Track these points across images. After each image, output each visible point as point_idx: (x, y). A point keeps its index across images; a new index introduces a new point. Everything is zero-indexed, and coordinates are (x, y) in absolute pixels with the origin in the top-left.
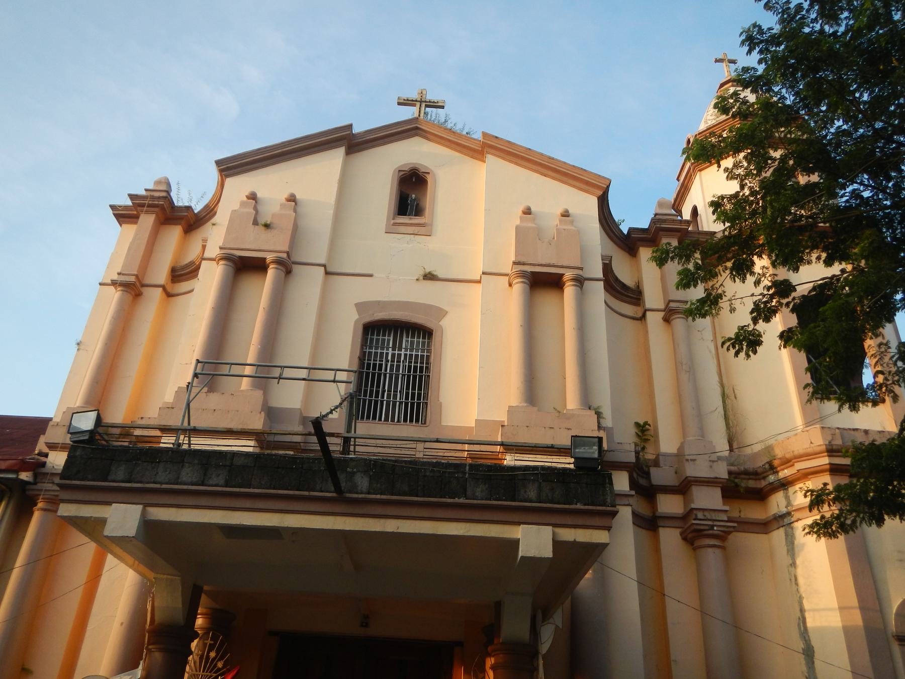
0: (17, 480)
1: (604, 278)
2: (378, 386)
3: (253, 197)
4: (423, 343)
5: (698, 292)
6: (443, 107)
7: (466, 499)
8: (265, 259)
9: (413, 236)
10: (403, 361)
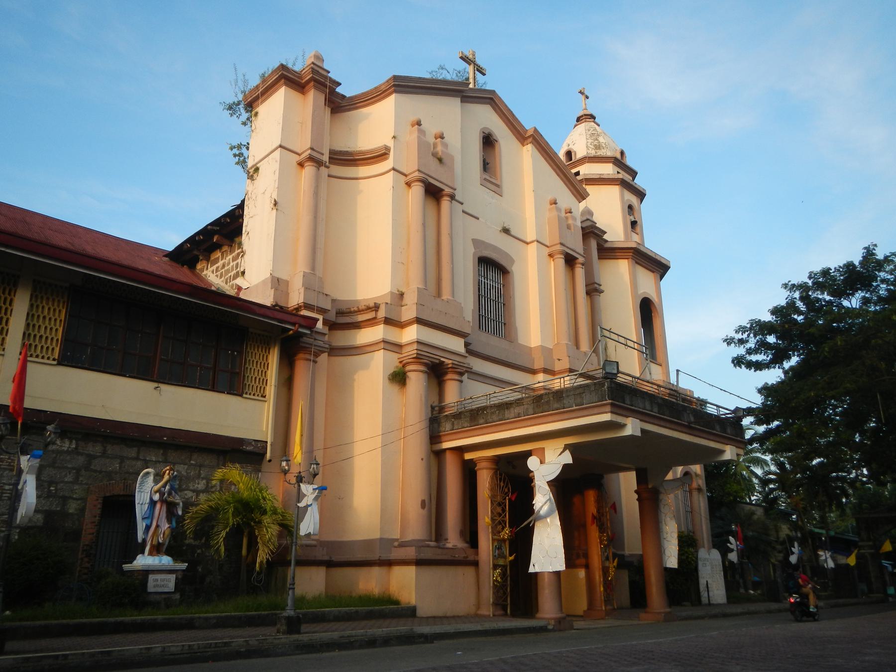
5: (739, 336)
6: (484, 74)
8: (442, 190)
9: (494, 193)
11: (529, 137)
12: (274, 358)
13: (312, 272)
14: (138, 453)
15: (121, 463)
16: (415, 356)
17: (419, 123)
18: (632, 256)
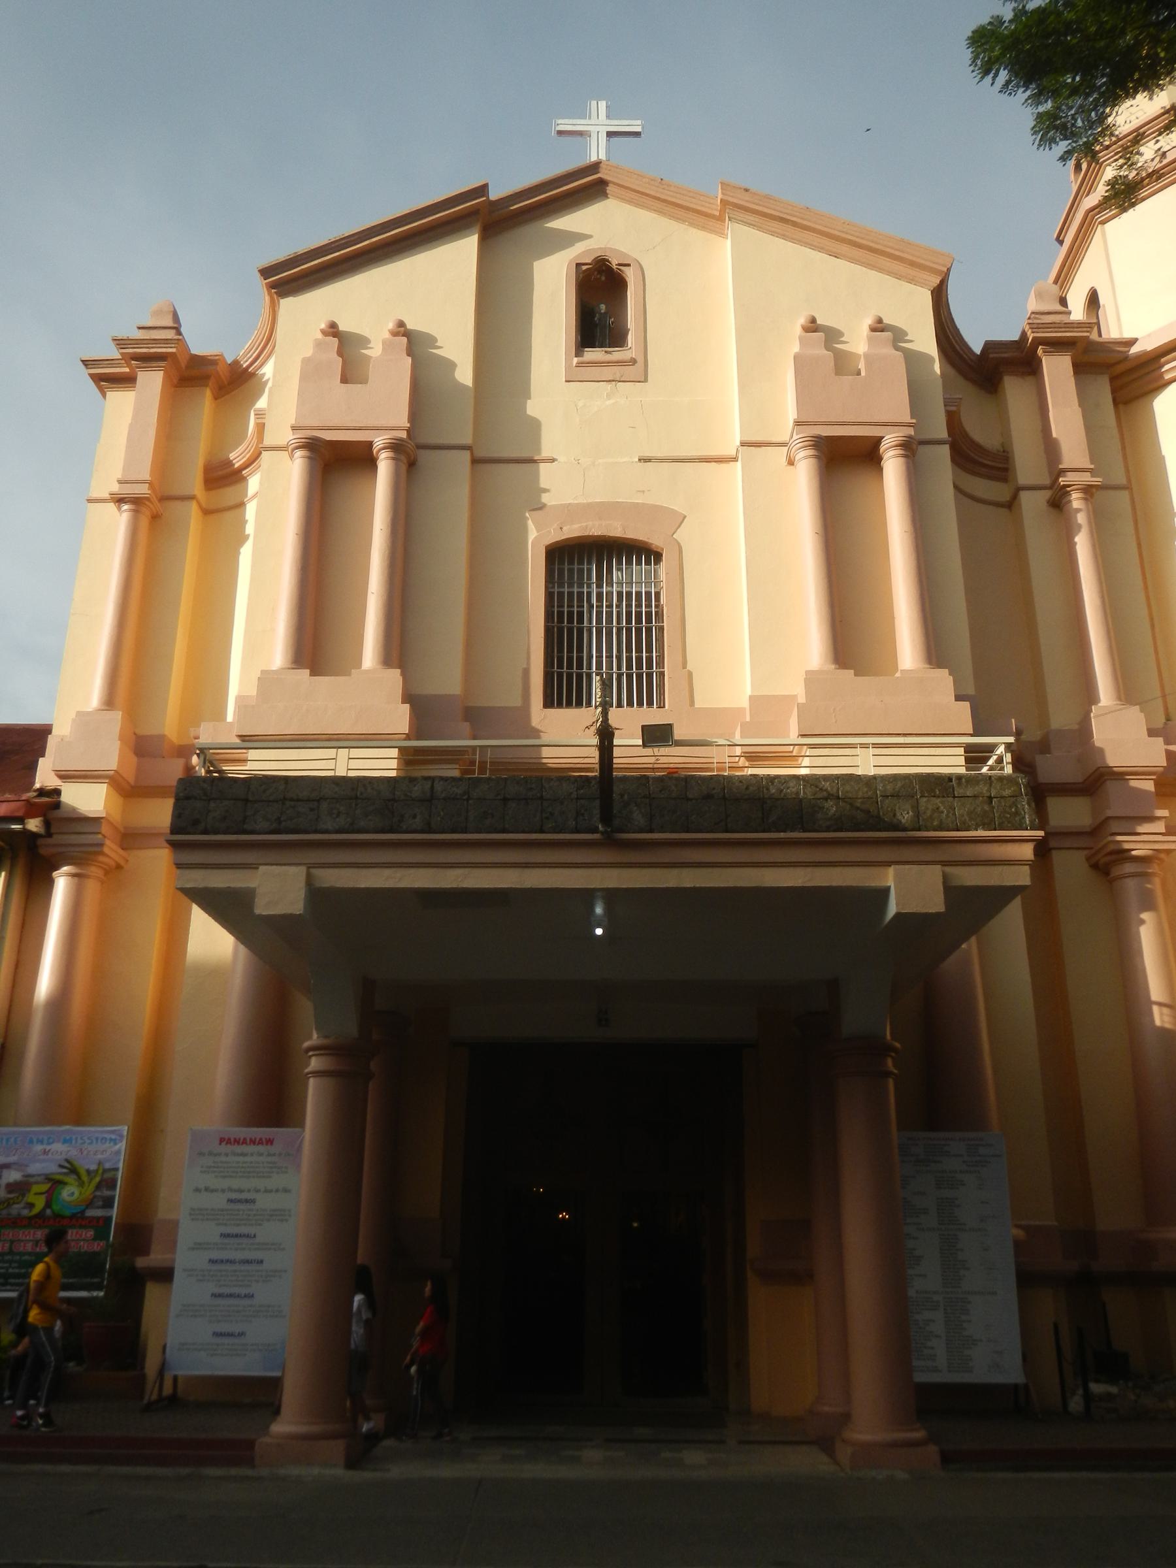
0: (26, 833)
1: (950, 439)
2: (580, 649)
3: (333, 330)
4: (648, 573)
7: (804, 831)
10: (617, 606)
11: (722, 211)
13: (109, 708)
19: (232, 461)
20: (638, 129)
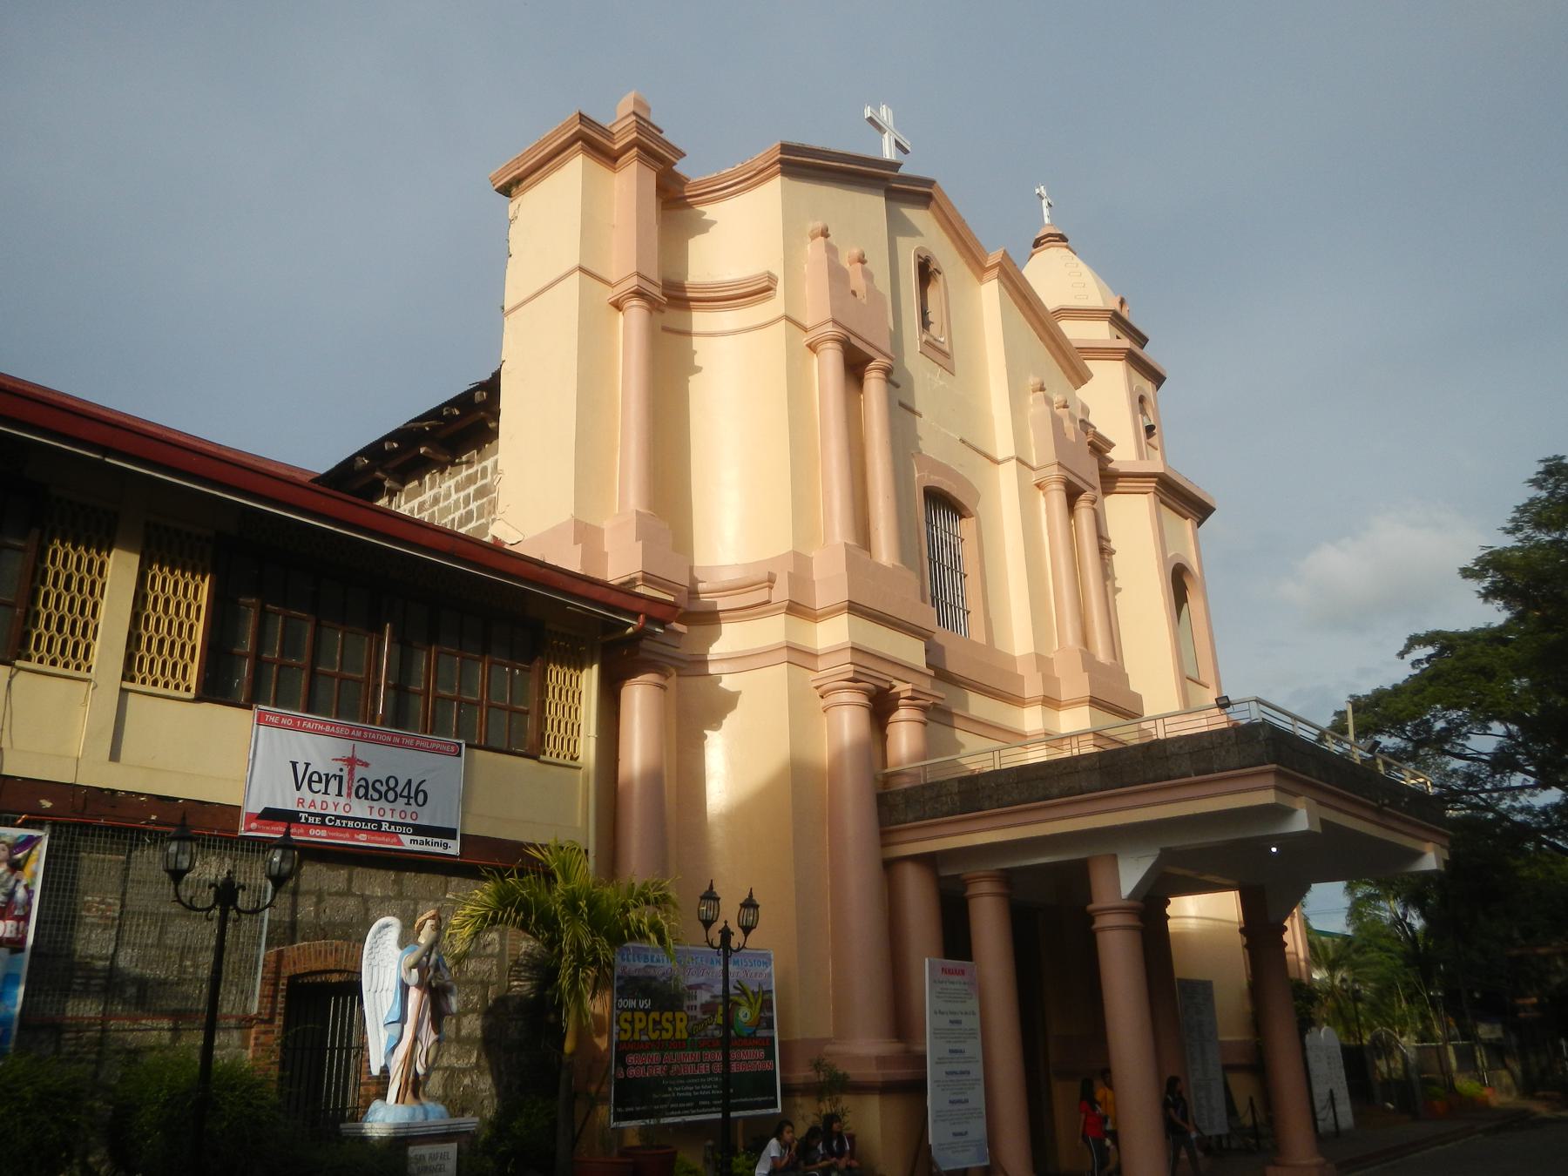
11: (992, 267)
12: (589, 680)
14: (350, 880)
15: (318, 904)
16: (851, 675)
17: (825, 233)
18: (1156, 488)
19: (685, 288)
20: (909, 149)
